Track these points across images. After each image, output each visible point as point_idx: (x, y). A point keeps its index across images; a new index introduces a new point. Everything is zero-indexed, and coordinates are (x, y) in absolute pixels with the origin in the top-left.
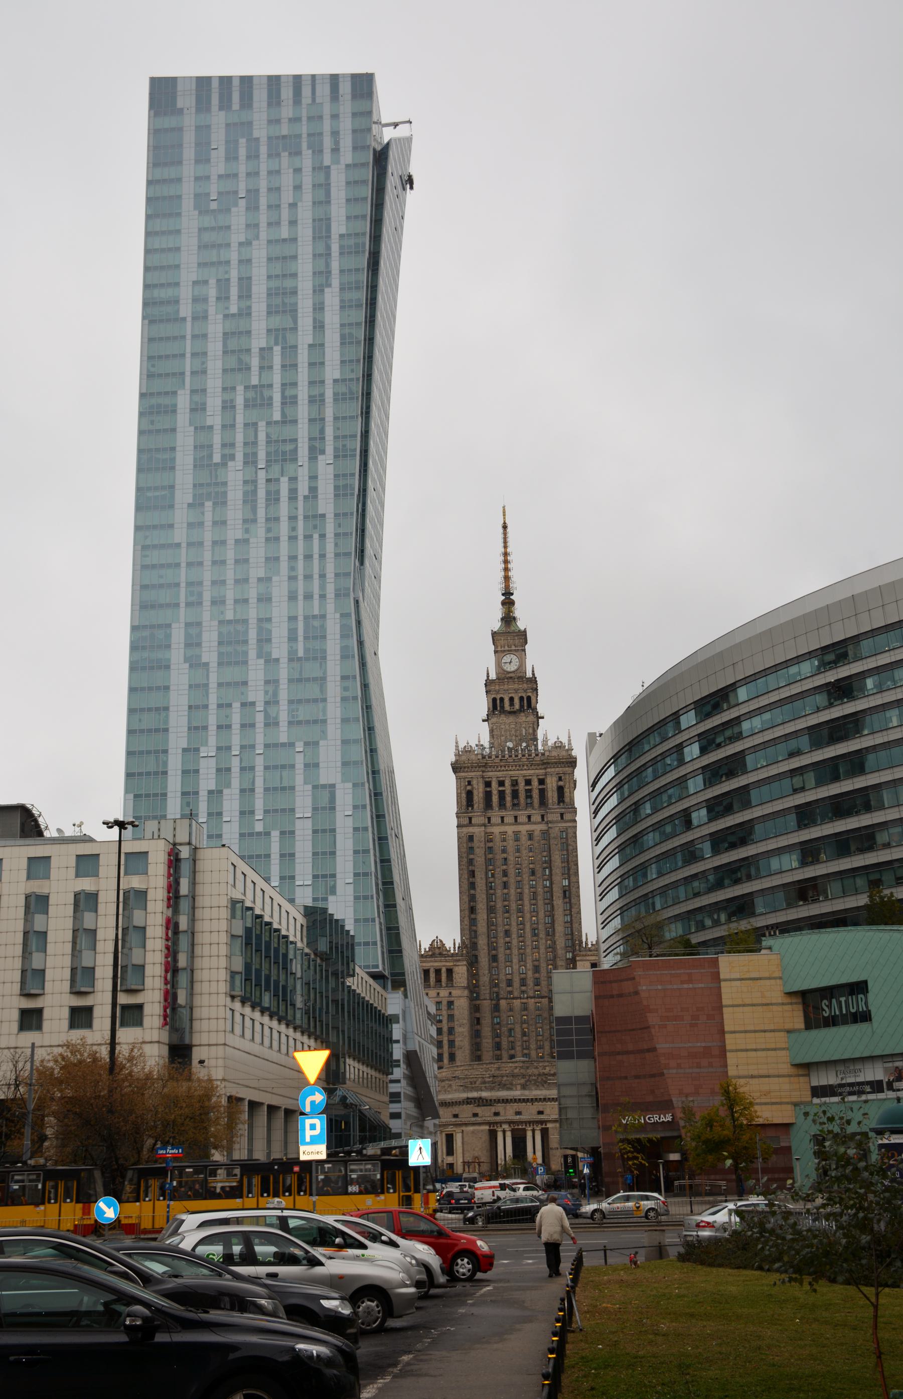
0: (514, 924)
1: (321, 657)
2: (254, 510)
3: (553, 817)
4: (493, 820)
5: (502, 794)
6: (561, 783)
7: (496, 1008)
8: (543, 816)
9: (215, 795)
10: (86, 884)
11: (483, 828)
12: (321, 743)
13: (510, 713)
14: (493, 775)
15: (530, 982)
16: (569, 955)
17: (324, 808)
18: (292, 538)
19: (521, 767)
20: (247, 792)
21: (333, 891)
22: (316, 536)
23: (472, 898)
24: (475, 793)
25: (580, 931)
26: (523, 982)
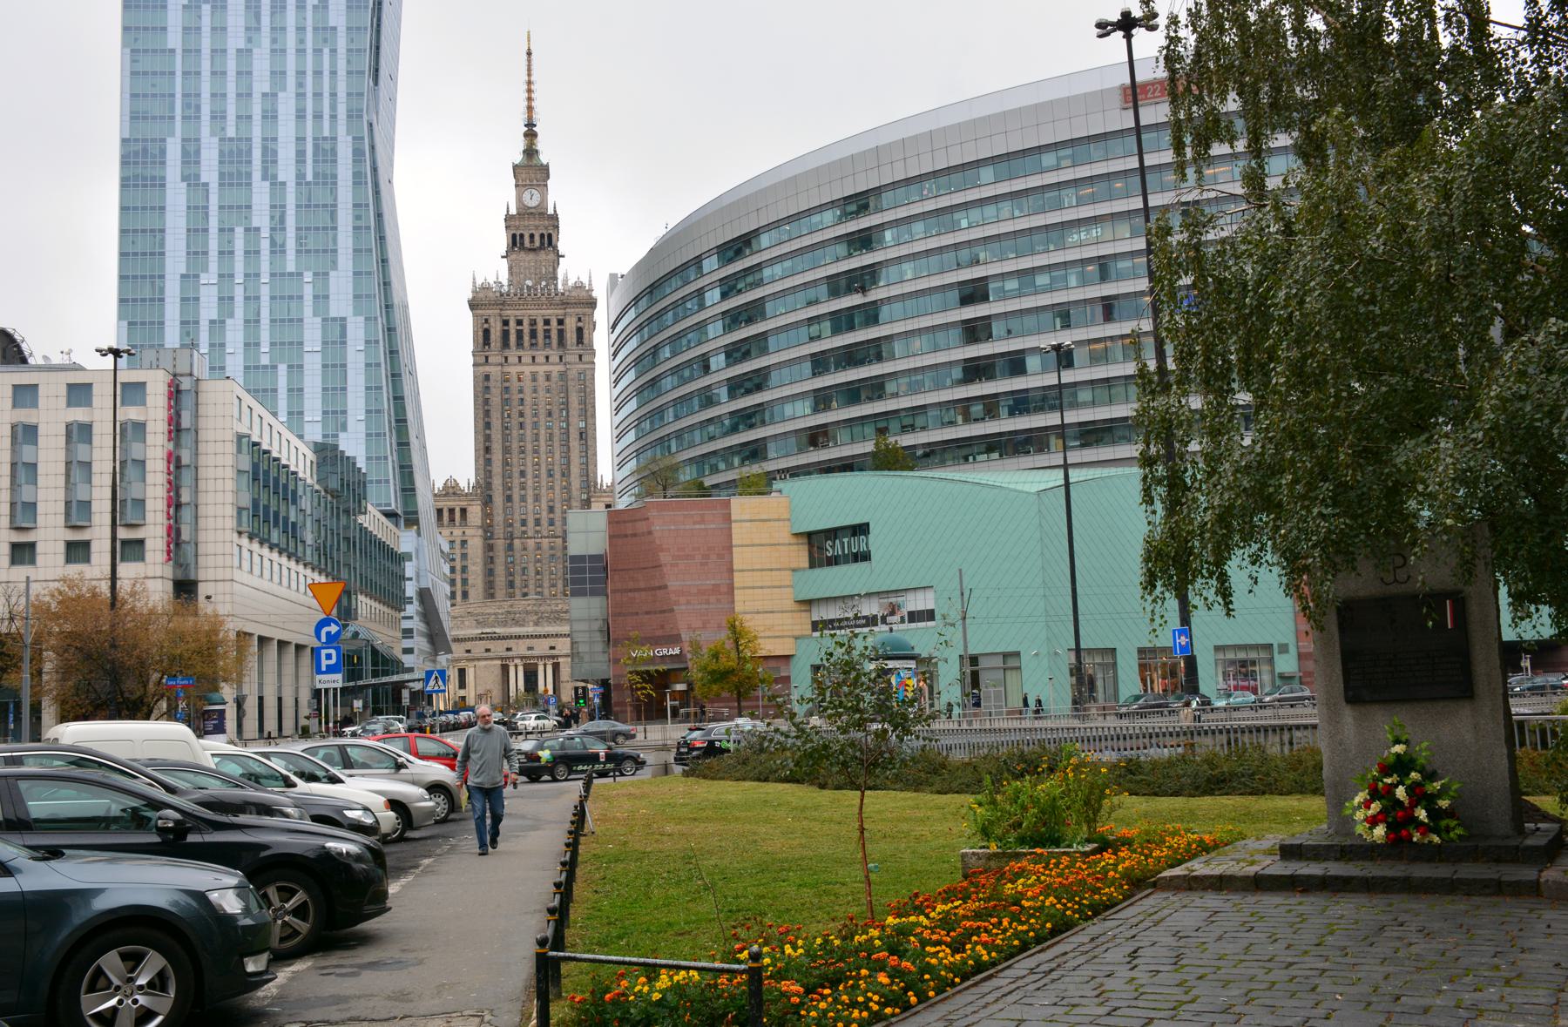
0: (529, 464)
1: (331, 181)
2: (258, 17)
3: (571, 358)
5: (520, 334)
7: (510, 547)
9: (217, 325)
10: (79, 415)
12: (332, 273)
14: (511, 314)
15: (545, 522)
16: (584, 497)
17: (334, 343)
18: (301, 52)
19: (540, 306)
20: (252, 323)
21: (344, 428)
22: (326, 51)
23: (488, 438)
25: (595, 474)
26: (538, 522)
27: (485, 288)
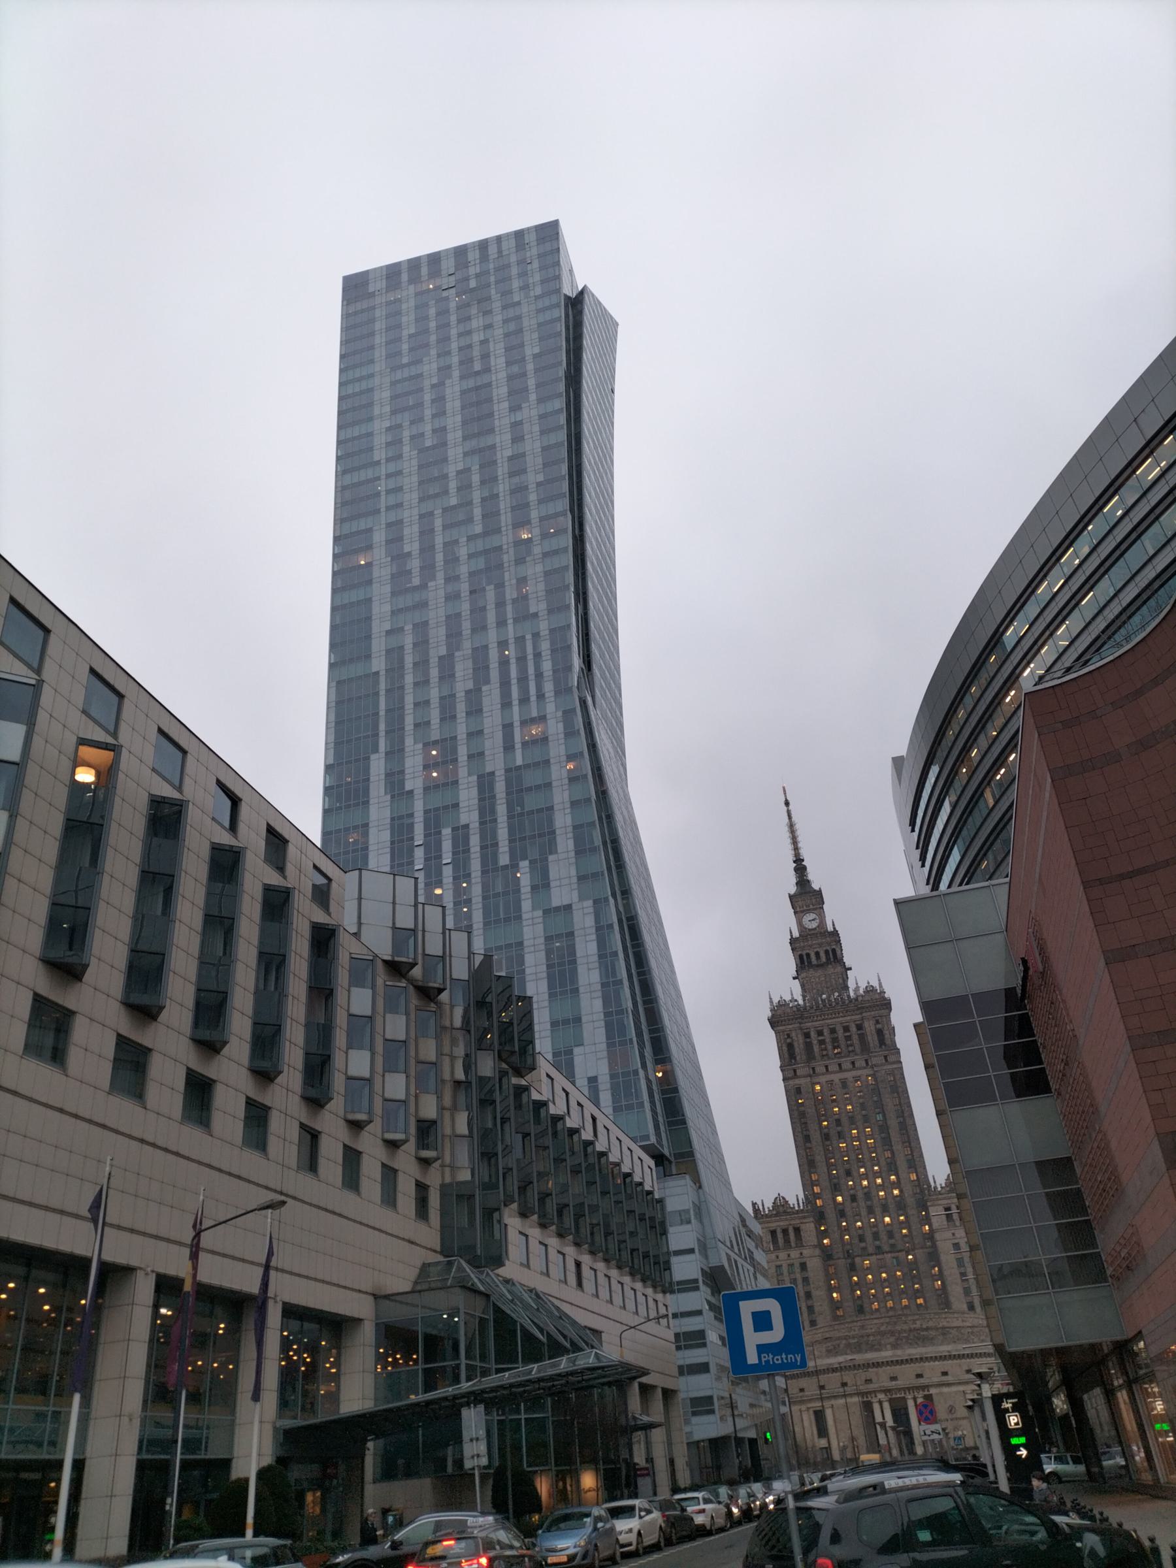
4: (818, 1070)
6: (879, 1026)
8: (866, 1061)
11: (808, 1079)
13: (818, 966)
24: (796, 1044)
27: (782, 1004)
